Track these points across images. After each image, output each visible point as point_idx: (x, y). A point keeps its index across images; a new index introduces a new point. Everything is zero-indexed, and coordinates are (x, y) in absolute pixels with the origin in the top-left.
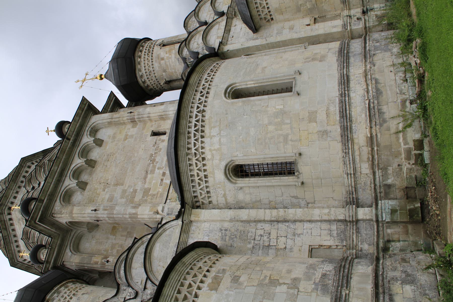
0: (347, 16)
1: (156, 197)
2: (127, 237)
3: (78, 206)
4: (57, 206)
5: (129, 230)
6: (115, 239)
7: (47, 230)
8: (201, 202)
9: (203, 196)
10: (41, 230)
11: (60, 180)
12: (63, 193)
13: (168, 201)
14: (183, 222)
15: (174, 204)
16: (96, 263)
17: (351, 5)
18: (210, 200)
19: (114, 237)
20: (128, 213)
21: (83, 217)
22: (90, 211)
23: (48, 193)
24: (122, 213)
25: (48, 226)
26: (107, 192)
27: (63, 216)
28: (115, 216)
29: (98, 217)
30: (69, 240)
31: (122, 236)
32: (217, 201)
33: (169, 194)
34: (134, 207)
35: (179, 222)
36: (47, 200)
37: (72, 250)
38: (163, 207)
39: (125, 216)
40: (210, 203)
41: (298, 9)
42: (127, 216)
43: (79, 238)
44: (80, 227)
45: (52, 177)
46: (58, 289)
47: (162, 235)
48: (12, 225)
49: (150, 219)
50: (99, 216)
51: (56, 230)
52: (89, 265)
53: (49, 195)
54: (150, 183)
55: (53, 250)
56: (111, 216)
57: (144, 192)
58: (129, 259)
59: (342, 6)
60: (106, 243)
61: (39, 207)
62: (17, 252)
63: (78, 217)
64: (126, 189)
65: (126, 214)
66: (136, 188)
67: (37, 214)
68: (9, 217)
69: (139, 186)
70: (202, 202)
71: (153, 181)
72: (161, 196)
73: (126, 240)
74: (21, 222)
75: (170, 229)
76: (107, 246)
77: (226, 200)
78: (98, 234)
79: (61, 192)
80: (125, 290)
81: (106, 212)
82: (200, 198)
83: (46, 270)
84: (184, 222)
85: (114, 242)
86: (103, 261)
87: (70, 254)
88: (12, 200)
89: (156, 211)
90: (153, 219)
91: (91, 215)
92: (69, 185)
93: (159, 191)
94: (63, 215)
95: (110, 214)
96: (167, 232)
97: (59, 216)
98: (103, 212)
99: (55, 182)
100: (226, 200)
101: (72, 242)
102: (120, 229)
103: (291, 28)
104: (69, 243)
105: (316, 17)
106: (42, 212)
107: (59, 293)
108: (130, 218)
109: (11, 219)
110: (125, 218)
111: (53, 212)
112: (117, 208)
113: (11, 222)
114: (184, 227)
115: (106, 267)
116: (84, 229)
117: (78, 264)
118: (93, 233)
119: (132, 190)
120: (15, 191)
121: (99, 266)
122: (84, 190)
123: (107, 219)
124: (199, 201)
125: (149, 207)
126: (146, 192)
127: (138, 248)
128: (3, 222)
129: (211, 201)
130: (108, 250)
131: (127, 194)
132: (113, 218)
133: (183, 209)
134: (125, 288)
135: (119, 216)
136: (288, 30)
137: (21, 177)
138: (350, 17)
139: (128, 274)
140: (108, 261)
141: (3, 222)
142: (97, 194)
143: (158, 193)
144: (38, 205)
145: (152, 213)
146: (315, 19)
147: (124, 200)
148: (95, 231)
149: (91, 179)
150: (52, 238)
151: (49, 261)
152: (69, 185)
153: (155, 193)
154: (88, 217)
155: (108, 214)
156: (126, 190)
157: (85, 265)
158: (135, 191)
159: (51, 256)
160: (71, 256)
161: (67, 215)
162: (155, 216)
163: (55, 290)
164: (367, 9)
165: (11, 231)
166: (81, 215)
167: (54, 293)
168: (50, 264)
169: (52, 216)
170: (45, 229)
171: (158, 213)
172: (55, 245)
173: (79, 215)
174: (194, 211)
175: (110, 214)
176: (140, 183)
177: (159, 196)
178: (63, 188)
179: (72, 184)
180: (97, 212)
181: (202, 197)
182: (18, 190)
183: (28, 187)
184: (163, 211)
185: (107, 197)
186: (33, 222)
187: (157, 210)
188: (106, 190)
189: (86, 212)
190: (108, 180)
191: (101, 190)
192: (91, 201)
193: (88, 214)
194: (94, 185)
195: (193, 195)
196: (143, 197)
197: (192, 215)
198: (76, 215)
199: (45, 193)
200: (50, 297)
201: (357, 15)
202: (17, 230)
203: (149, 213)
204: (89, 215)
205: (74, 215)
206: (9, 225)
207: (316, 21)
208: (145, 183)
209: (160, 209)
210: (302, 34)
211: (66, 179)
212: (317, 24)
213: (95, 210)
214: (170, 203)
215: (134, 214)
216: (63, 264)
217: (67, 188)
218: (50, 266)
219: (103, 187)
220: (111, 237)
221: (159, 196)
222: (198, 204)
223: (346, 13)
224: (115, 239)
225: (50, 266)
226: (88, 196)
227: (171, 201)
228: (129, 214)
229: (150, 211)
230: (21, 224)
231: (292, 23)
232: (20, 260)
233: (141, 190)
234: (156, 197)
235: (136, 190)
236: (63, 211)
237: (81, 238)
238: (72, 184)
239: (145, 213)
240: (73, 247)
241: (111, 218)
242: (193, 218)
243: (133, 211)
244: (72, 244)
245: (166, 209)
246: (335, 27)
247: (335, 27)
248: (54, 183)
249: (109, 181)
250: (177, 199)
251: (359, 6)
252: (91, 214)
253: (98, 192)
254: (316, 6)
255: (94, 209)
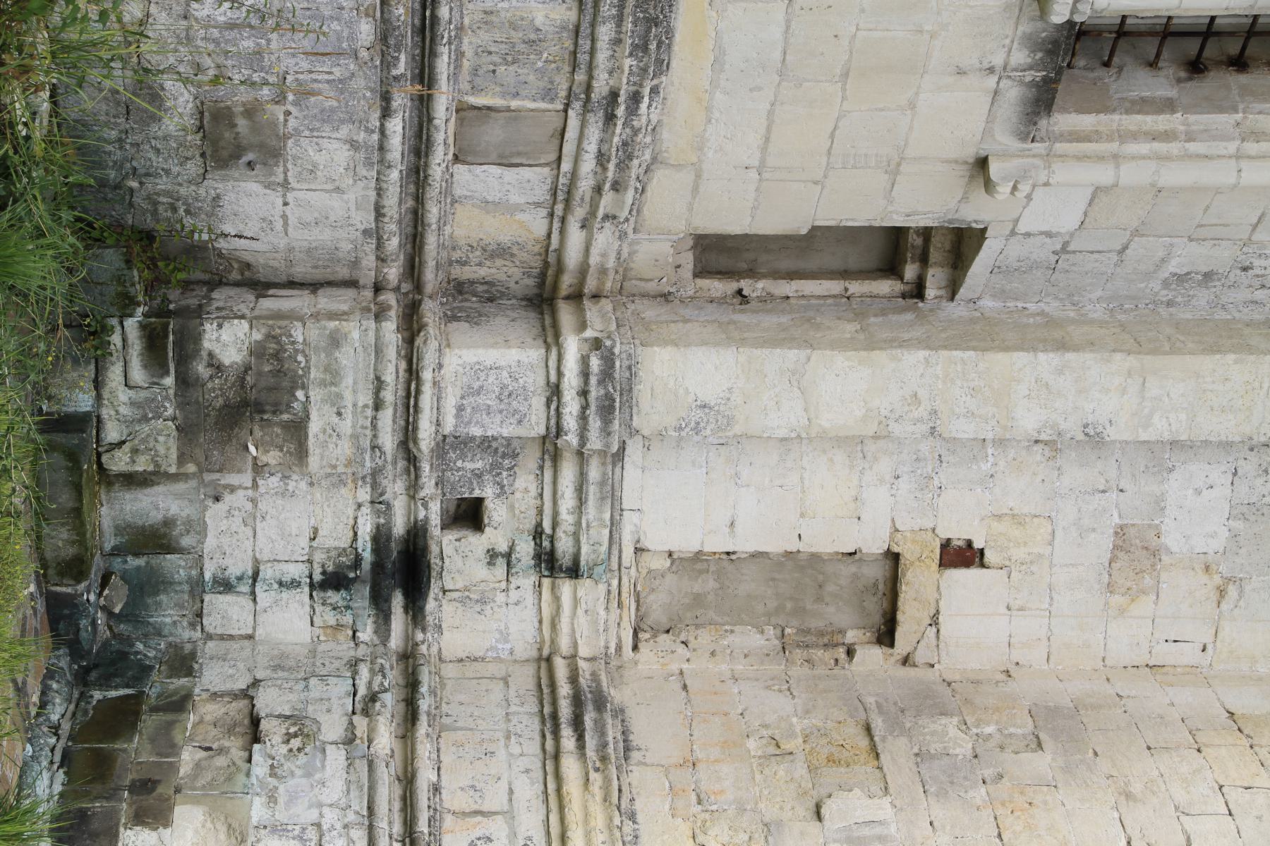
0: (574, 572)
17: (524, 679)
41: (1059, 726)
59: (617, 695)
103: (1135, 553)
105: (871, 657)
136: (1172, 540)
138: (549, 562)
146: (886, 634)
164: (380, 602)
201: (480, 572)
207: (875, 607)
210: (1035, 388)
212: (875, 545)
223: (588, 619)
231: (1128, 637)
246: (710, 429)
247: (710, 429)
251: (449, 671)
254: (878, 724)
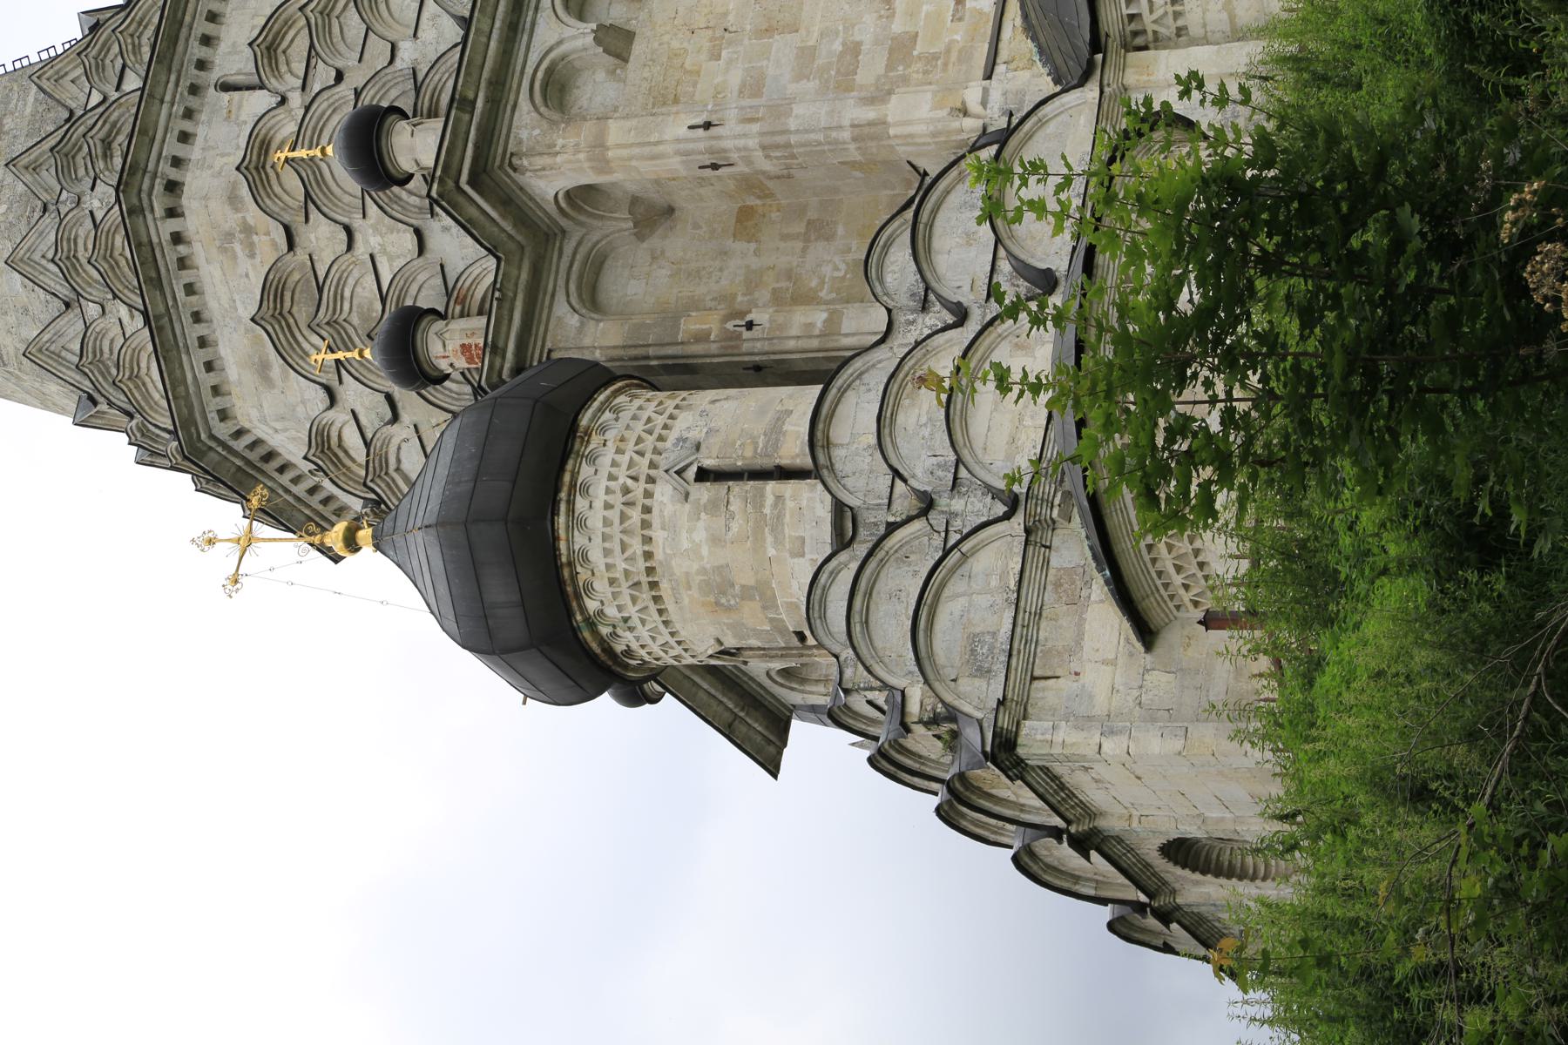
1: (946, 64)
2: (807, 240)
3: (627, 117)
4: (526, 122)
5: (812, 214)
6: (757, 253)
7: (487, 224)
8: (1150, 34)
9: (1158, 13)
10: (469, 221)
11: (513, 29)
12: (540, 75)
13: (1000, 69)
14: (1102, 92)
15: (1024, 75)
16: (702, 337)
18: (1180, 23)
19: (753, 246)
20: (846, 123)
21: (654, 157)
22: (683, 131)
23: (486, 74)
24: (823, 124)
25: (494, 207)
26: (730, 62)
27: (559, 159)
28: (793, 139)
29: (725, 151)
30: (557, 272)
31: (785, 237)
32: (1205, 25)
33: (1003, 45)
34: (871, 101)
35: (1090, 92)
36: (487, 101)
37: (577, 307)
38: (986, 91)
39: (834, 134)
40: (1178, 35)
42: (846, 135)
43: (595, 266)
44: (602, 217)
45: (489, 9)
46: (608, 399)
47: (1035, 138)
48: (182, 263)
49: (934, 135)
50: (728, 144)
51: (515, 226)
52: (670, 351)
53: (490, 83)
54: (912, 14)
55: (507, 305)
56: (780, 139)
57: (891, 51)
58: (921, 227)
60: (721, 270)
61: (463, 129)
62: (206, 393)
63: (631, 158)
64: (811, 43)
65: (840, 127)
66: (858, 39)
67: (458, 153)
68: (173, 225)
69: (867, 30)
70: (1155, 32)
71: (925, 8)
72: (965, 56)
73: (804, 250)
74: (238, 247)
75: (1059, 119)
76: (724, 282)
77: (1232, 18)
78: (675, 243)
79: (529, 70)
80: (912, 323)
81: (755, 127)
82: (1148, 19)
83: (495, 379)
84: (1107, 90)
85: (755, 263)
86: (730, 326)
87: (574, 320)
88: (172, 147)
89: (959, 105)
90: (949, 133)
91: (691, 146)
92: (560, 43)
93: (952, 42)
94: (551, 164)
95: (773, 133)
96: (1051, 128)
97: (539, 162)
98: (739, 129)
99: (501, 29)
100: (1232, 18)
101: (574, 277)
102: (775, 215)
104: (561, 282)
106: (477, 147)
107: (617, 411)
108: (854, 139)
109: (177, 238)
110: (836, 142)
111: (511, 148)
112: (798, 110)
113: (182, 249)
114: (1105, 106)
115: (746, 347)
116: (620, 224)
117: (621, 352)
118: (655, 242)
119: (837, 46)
120: (178, 109)
121: (714, 348)
122: (626, 61)
123: (760, 153)
124: (1144, 32)
125: (929, 96)
126: (901, 49)
127: (947, 192)
128: (146, 250)
129: (1186, 28)
130: (734, 296)
131: (819, 62)
132: (788, 145)
133: (1099, 57)
134: (911, 318)
135: (812, 136)
137: (194, 45)
139: (925, 266)
140: (750, 325)
141: (146, 250)
142: (686, 72)
143: (948, 51)
144: (457, 119)
145: (944, 113)
147: (811, 85)
148: (660, 231)
149: (643, 15)
150: (498, 259)
151: (501, 344)
152: (560, 43)
153: (939, 47)
154: (678, 153)
155: (762, 134)
156: (815, 48)
157: (651, 351)
158: (854, 49)
159: (504, 329)
160: (581, 329)
161: (581, 156)
162: (956, 125)
163: (603, 404)
165: (180, 294)
166: (647, 150)
167: (601, 410)
168: (504, 358)
169: (511, 165)
170: (482, 218)
171: (966, 113)
172: (511, 286)
173: (637, 150)
174: (1133, 57)
175: (773, 133)
176: (869, 19)
177: (954, 57)
178: (533, 58)
179: (574, 37)
180: (713, 131)
181: (1155, 16)
182: (193, 102)
183: (273, 80)
184: (984, 103)
185: (735, 78)
186: (450, 183)
187: (964, 103)
188: (724, 53)
189: (666, 137)
190: (725, 14)
191: (703, 57)
192: (664, 100)
193: (678, 141)
194: (666, 38)
195: (1125, 12)
196: (890, 67)
197: (1129, 71)
198: (625, 152)
199: (475, 76)
200: (592, 420)
202: (208, 289)
203: (932, 114)
204: (682, 146)
205: (610, 154)
206: (173, 266)
208: (891, 16)
209: (972, 96)
211: (540, 20)
213: (707, 125)
214: (1010, 75)
215: (870, 124)
216: (548, 357)
217: (552, 55)
218: (507, 366)
219: (707, 45)
220: (740, 246)
221: (954, 57)
222: (1139, 41)
224: (757, 253)
225: (507, 366)
226: (645, 85)
227: (1013, 66)
228: (853, 126)
229: (936, 106)
230: (235, 257)
232: (223, 430)
233: (876, 42)
234: (946, 64)
235: (858, 44)
236: (560, 142)
237: (602, 263)
238: (574, 37)
239: (920, 119)
240: (580, 296)
241: (777, 147)
242: (1131, 78)
243: (870, 114)
244: (572, 287)
245: (996, 98)
248: (501, 35)
249: (731, 18)
250: (1036, 58)
252: (687, 140)
253: (688, 65)
255: (699, 121)
